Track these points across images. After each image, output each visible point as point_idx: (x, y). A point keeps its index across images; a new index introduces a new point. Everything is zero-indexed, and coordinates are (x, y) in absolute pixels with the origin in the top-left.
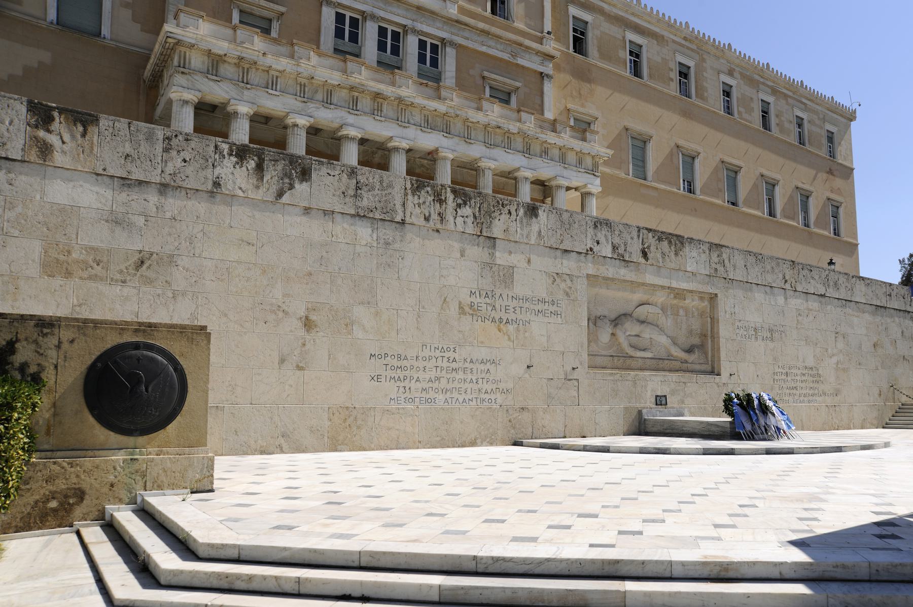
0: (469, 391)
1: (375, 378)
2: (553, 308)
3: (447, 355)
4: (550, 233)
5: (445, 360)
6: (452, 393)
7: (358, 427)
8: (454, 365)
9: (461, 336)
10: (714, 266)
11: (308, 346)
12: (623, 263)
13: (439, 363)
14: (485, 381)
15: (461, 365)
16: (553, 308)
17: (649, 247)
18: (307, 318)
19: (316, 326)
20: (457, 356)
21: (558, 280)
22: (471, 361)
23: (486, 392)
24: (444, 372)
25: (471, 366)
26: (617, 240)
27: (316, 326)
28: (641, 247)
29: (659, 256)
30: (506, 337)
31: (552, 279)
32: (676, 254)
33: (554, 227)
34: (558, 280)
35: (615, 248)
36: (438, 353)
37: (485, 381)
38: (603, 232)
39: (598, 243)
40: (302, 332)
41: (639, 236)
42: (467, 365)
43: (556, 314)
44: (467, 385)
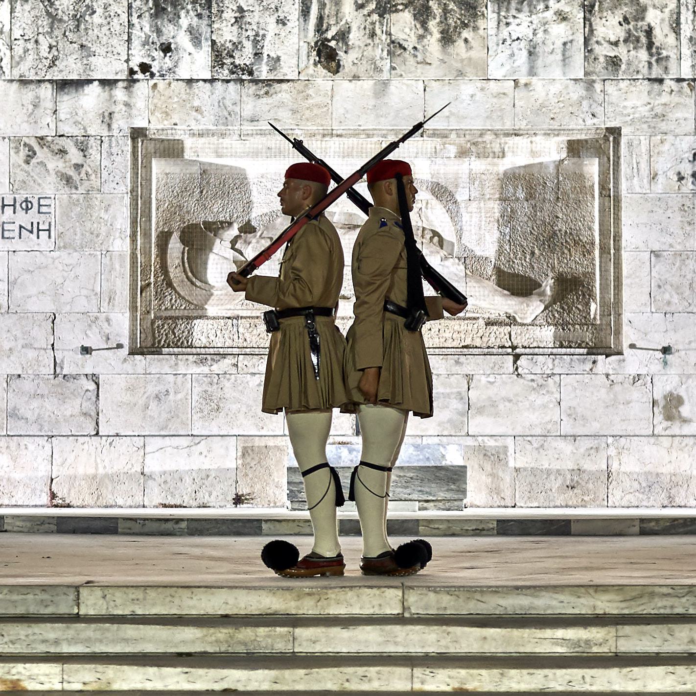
2: (23, 219)
4: (19, 50)
10: (603, 51)
12: (253, 88)
16: (23, 219)
17: (342, 36)
21: (42, 154)
26: (227, 33)
28: (311, 36)
29: (379, 52)
31: (23, 152)
32: (447, 39)
33: (29, 34)
34: (42, 154)
35: (219, 56)
38: (184, 22)
39: (166, 49)
41: (305, 12)
43: (35, 230)
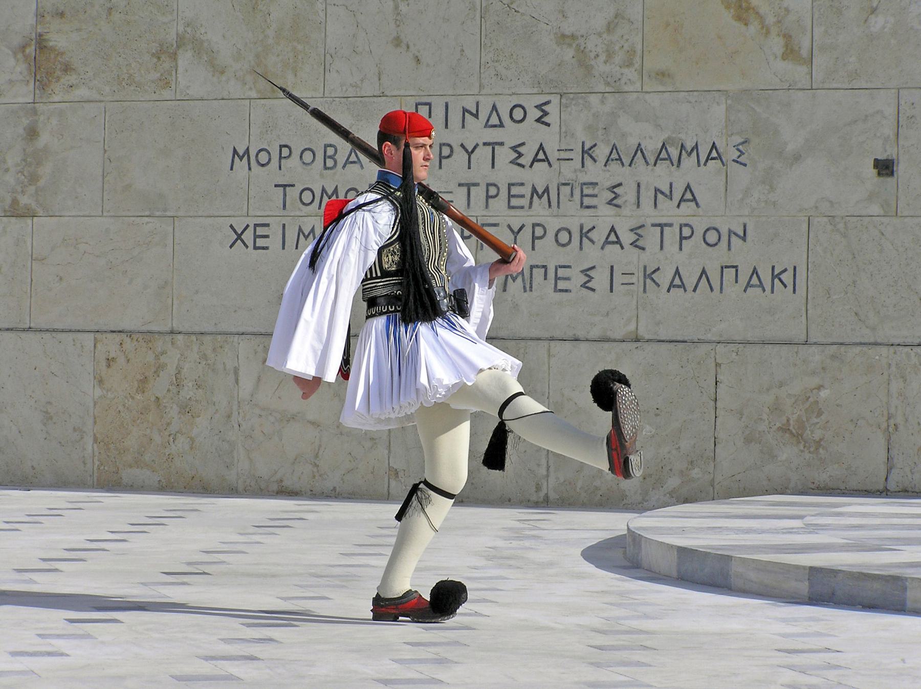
0: (600, 279)
1: (248, 236)
3: (510, 134)
5: (505, 155)
6: (528, 287)
7: (186, 409)
8: (539, 176)
9: (569, 54)
11: (44, 139)
13: (481, 170)
14: (671, 235)
15: (568, 171)
18: (41, 43)
19: (67, 68)
20: (551, 139)
22: (614, 157)
23: (677, 282)
24: (498, 205)
25: (617, 173)
27: (67, 68)
30: (776, 44)
36: (476, 133)
37: (671, 235)
40: (24, 94)
42: (594, 172)
44: (592, 254)
